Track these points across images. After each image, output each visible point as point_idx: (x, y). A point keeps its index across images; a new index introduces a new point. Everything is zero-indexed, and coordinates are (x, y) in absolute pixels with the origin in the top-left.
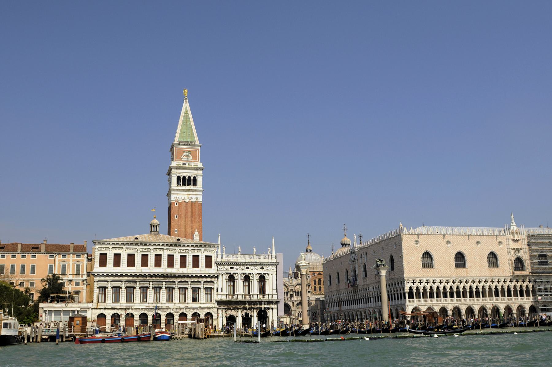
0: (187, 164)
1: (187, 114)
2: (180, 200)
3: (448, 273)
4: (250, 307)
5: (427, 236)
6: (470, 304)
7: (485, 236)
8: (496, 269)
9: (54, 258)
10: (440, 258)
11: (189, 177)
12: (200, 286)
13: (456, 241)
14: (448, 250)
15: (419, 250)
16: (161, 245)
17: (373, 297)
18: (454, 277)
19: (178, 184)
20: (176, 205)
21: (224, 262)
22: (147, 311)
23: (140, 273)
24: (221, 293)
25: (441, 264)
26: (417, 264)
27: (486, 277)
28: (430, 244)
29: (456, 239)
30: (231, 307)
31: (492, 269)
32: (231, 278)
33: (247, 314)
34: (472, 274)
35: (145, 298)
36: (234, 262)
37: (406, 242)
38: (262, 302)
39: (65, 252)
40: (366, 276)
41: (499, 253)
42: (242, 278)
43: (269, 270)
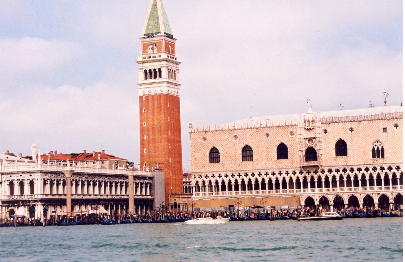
0: (152, 57)
1: (156, 4)
2: (147, 94)
7: (275, 128)
10: (226, 153)
11: (155, 70)
13: (243, 135)
14: (235, 144)
15: (206, 146)
18: (238, 171)
19: (146, 78)
28: (217, 140)
38: (30, 200)
41: (290, 144)
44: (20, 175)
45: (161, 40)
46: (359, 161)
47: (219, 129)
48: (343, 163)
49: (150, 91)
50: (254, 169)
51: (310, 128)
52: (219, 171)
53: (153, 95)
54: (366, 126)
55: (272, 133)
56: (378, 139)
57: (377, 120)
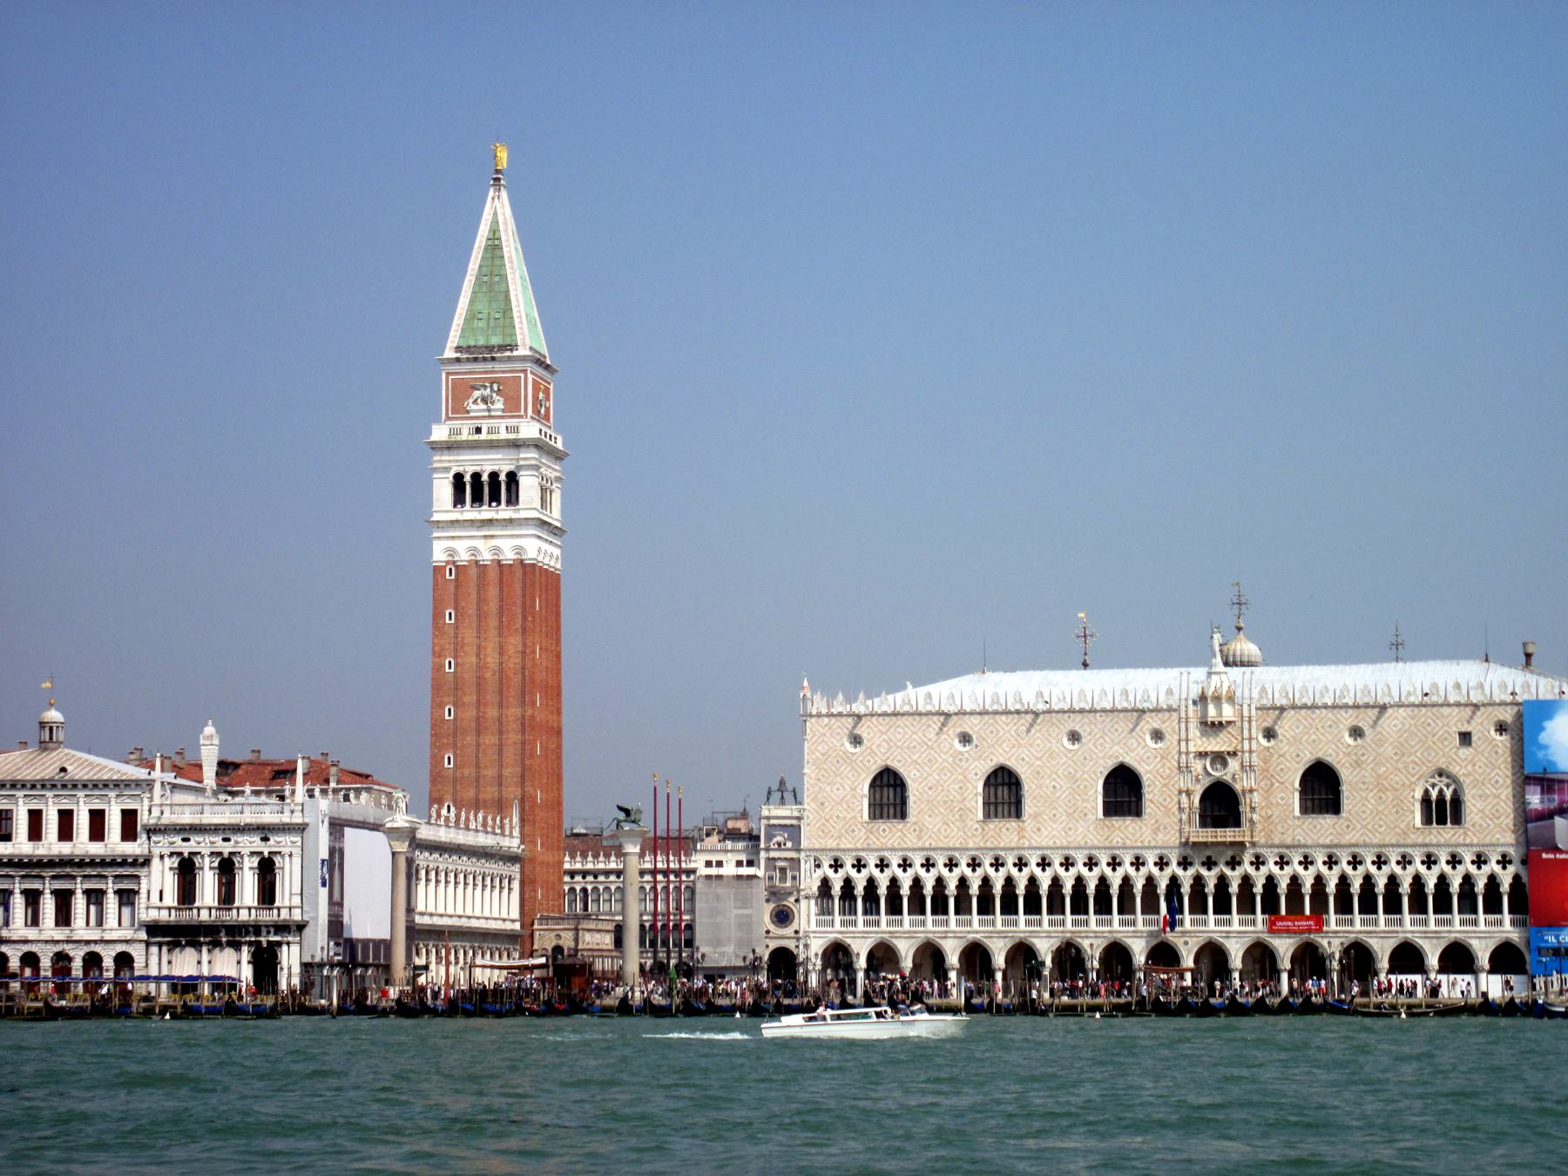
0: (484, 430)
1: (497, 242)
2: (464, 557)
6: (1022, 935)
7: (1098, 714)
8: (1128, 822)
10: (930, 788)
11: (494, 476)
12: (103, 886)
13: (992, 732)
14: (961, 760)
19: (459, 500)
20: (451, 574)
24: (159, 904)
28: (899, 744)
29: (992, 725)
32: (187, 870)
34: (1039, 840)
36: (188, 825)
38: (260, 926)
41: (1148, 768)
46: (1380, 833)
47: (907, 708)
48: (1327, 838)
49: (474, 551)
50: (1027, 845)
51: (1220, 723)
54: (1406, 722)
55: (1089, 730)
56: (1444, 766)
57: (1442, 705)
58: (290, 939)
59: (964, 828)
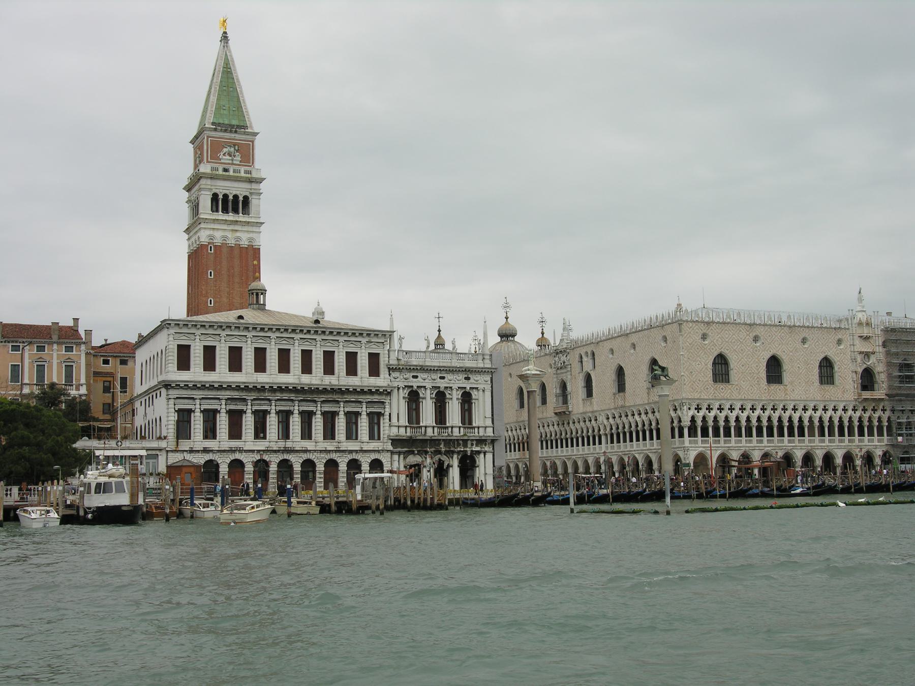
1: (229, 70)
2: (218, 241)
3: (755, 393)
4: (448, 449)
5: (722, 327)
6: (789, 448)
7: (816, 329)
8: (831, 387)
9: (20, 352)
10: (743, 366)
11: (236, 197)
12: (359, 410)
13: (770, 336)
14: (756, 351)
16: (290, 330)
17: (606, 435)
18: (764, 400)
19: (214, 209)
21: (403, 365)
22: (192, 457)
23: (254, 383)
25: (743, 377)
26: (704, 375)
27: (817, 401)
28: (727, 340)
30: (414, 449)
31: (826, 387)
32: (414, 398)
33: (441, 463)
35: (260, 431)
37: (688, 336)
38: (468, 440)
39: (43, 341)
40: (590, 394)
41: (838, 359)
42: (432, 396)
43: (480, 381)
44: (439, 375)
45: (250, 141)
47: (729, 320)
49: (225, 238)
52: (734, 399)
53: (232, 245)
58: (486, 449)
59: (760, 388)
